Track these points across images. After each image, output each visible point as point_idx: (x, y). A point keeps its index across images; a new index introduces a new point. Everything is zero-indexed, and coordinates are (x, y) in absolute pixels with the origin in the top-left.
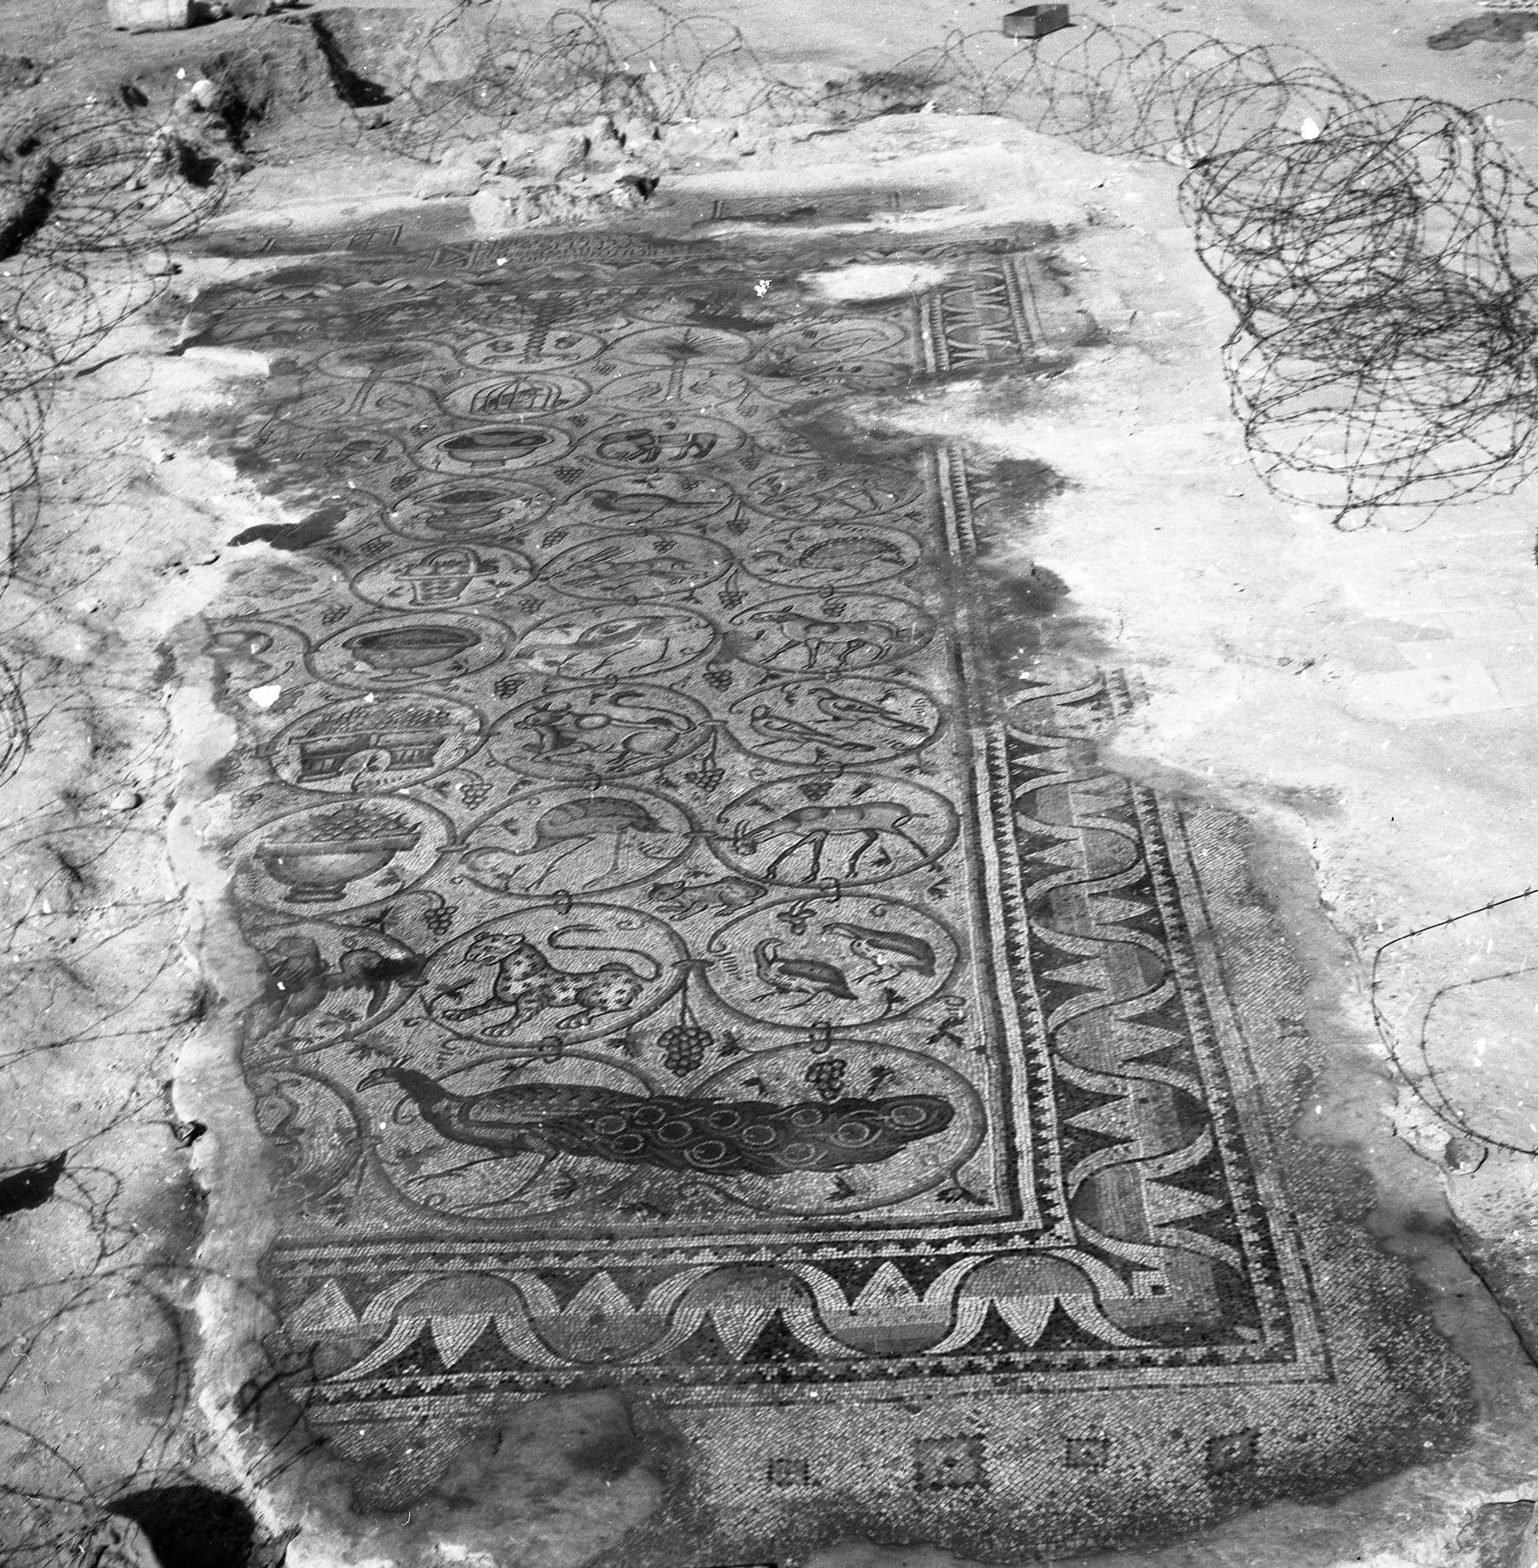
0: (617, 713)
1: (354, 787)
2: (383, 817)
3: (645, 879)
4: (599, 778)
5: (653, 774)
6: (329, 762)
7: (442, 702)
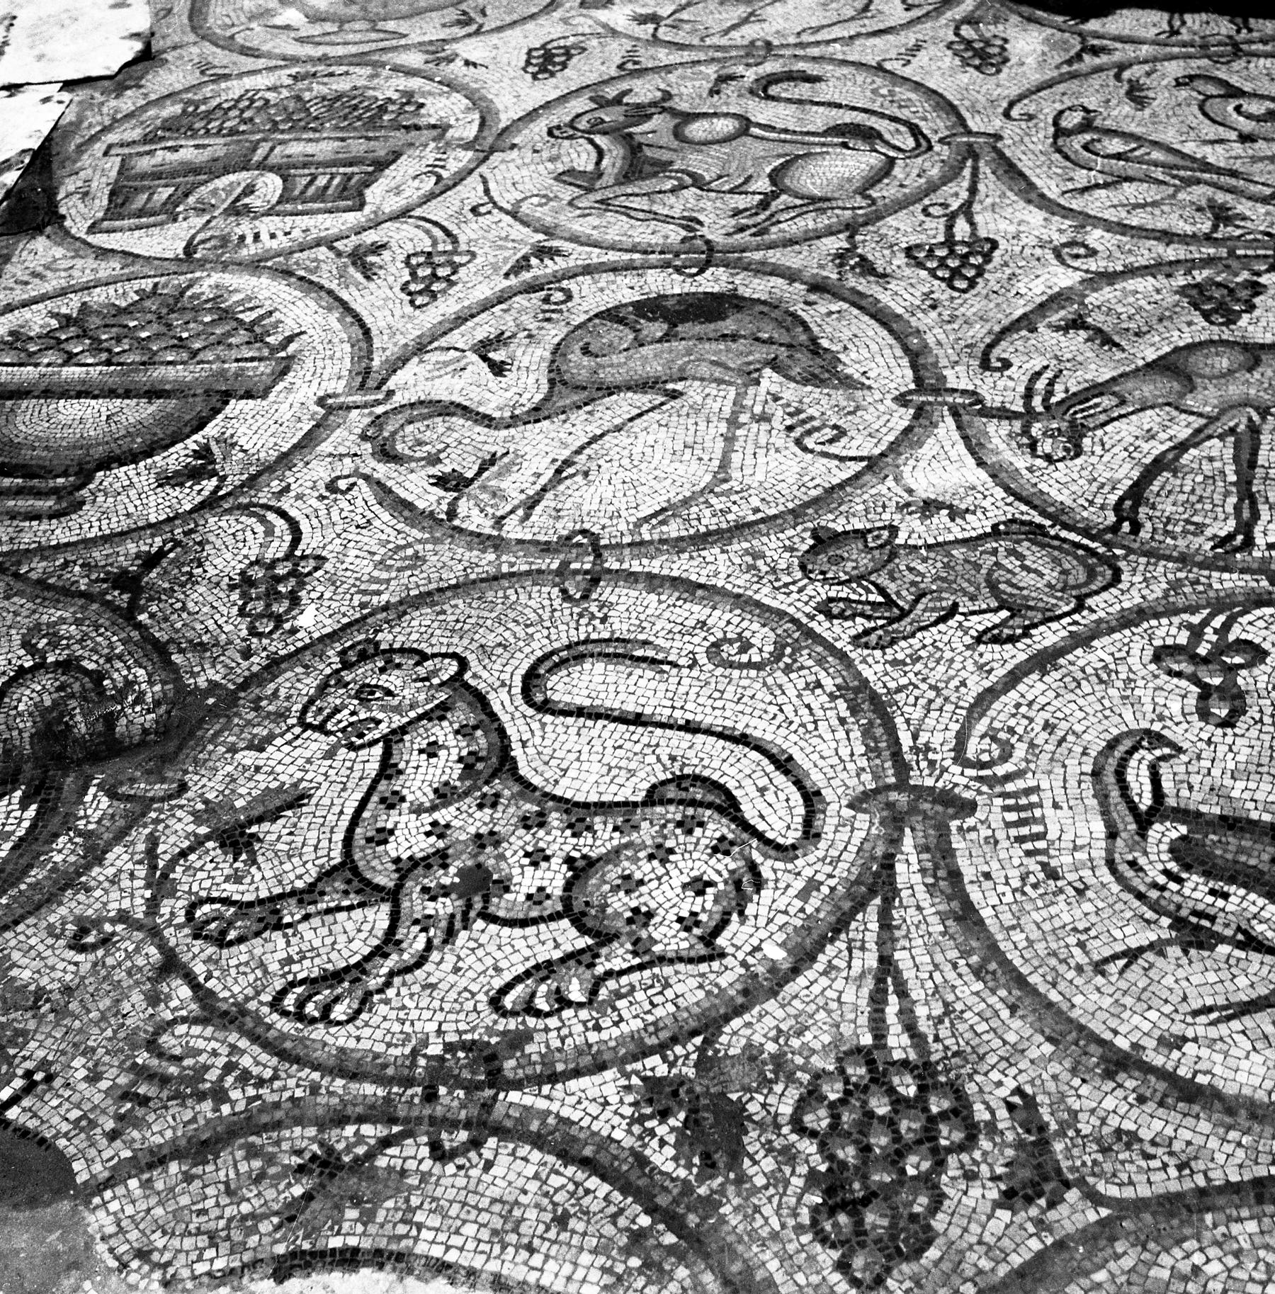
0: (762, 113)
1: (190, 249)
2: (226, 315)
3: (797, 514)
5: (836, 243)
6: (164, 193)
7: (415, 83)
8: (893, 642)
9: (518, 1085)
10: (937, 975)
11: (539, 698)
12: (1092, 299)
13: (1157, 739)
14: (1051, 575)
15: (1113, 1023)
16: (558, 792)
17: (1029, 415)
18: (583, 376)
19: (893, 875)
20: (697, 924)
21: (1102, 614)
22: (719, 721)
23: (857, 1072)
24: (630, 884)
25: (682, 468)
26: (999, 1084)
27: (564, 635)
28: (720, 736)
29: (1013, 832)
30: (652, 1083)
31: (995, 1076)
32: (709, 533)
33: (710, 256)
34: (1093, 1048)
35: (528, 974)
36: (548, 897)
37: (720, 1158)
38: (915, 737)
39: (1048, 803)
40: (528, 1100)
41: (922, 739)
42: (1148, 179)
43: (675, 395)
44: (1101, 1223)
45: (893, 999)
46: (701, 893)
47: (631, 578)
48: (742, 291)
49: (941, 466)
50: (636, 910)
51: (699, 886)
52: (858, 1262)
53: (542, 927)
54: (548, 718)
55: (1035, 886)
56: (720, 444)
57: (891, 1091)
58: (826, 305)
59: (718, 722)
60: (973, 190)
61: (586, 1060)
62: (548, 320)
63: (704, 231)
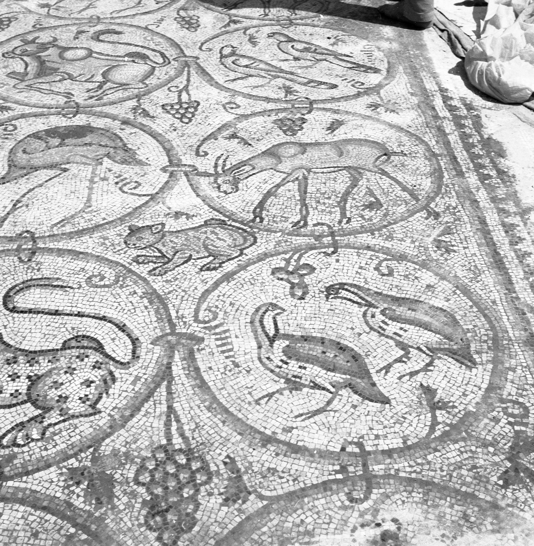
3: (122, 220)
4: (78, 105)
5: (133, 103)
8: (166, 272)
9: (11, 478)
10: (192, 412)
11: (11, 306)
12: (239, 126)
13: (274, 306)
14: (229, 241)
15: (264, 424)
16: (22, 347)
17: (217, 175)
18: (24, 163)
19: (171, 372)
20: (88, 400)
21: (250, 256)
22: (93, 311)
23: (161, 456)
24: (57, 385)
25: (70, 202)
26: (220, 454)
27: (21, 277)
28: (94, 317)
29: (220, 349)
30: (72, 471)
31: (218, 451)
32: (84, 230)
33: (78, 110)
34: (258, 436)
35: (13, 429)
36: (20, 394)
37: (104, 499)
38: (177, 312)
39: (233, 336)
40: (17, 484)
41: (180, 313)
42: (259, 76)
43: (65, 170)
44: (264, 507)
45: (174, 423)
46: (89, 386)
47: (50, 251)
48: (92, 124)
49: (182, 197)
50: (60, 396)
51: (88, 383)
52: (166, 536)
53: (18, 407)
54: (16, 315)
55: (230, 371)
56: (87, 191)
57: (175, 462)
58: (129, 130)
59: (92, 312)
60: (188, 80)
61: (42, 464)
62: (7, 138)
63: (74, 98)
